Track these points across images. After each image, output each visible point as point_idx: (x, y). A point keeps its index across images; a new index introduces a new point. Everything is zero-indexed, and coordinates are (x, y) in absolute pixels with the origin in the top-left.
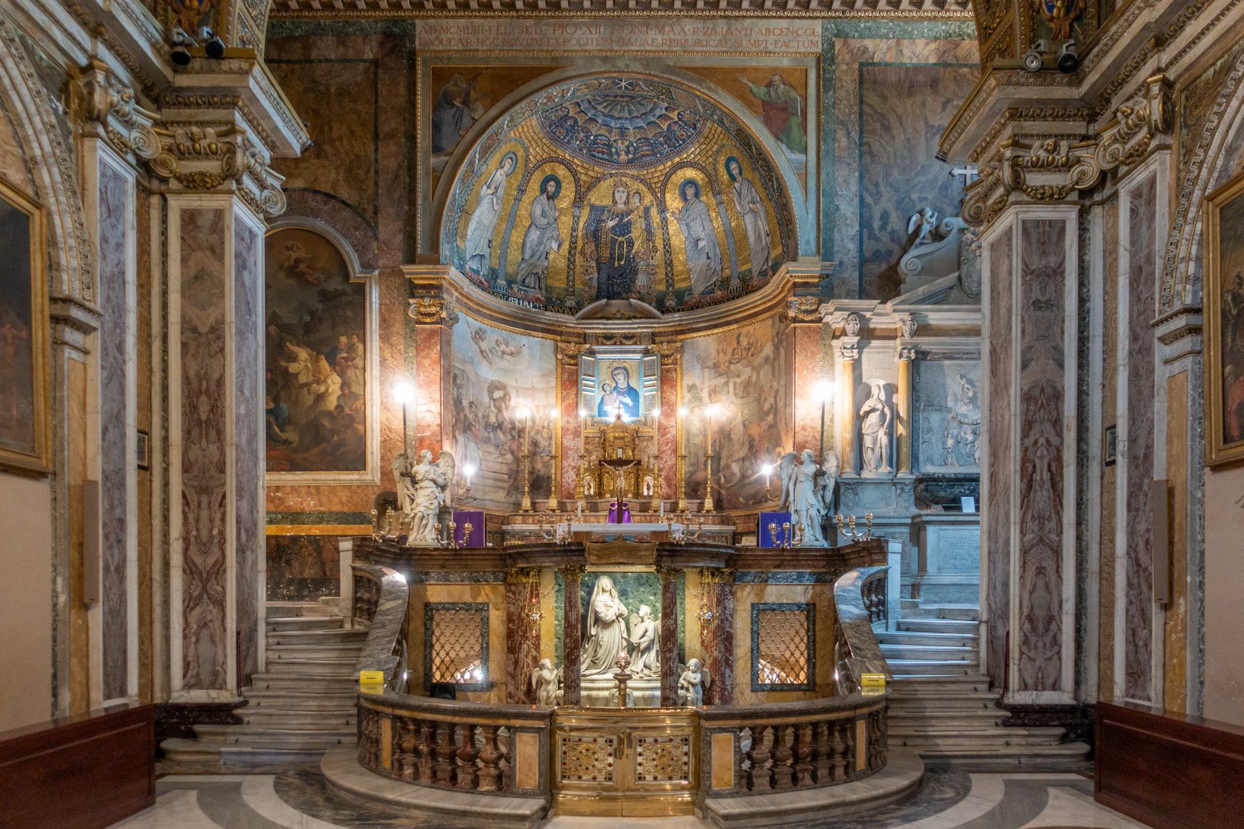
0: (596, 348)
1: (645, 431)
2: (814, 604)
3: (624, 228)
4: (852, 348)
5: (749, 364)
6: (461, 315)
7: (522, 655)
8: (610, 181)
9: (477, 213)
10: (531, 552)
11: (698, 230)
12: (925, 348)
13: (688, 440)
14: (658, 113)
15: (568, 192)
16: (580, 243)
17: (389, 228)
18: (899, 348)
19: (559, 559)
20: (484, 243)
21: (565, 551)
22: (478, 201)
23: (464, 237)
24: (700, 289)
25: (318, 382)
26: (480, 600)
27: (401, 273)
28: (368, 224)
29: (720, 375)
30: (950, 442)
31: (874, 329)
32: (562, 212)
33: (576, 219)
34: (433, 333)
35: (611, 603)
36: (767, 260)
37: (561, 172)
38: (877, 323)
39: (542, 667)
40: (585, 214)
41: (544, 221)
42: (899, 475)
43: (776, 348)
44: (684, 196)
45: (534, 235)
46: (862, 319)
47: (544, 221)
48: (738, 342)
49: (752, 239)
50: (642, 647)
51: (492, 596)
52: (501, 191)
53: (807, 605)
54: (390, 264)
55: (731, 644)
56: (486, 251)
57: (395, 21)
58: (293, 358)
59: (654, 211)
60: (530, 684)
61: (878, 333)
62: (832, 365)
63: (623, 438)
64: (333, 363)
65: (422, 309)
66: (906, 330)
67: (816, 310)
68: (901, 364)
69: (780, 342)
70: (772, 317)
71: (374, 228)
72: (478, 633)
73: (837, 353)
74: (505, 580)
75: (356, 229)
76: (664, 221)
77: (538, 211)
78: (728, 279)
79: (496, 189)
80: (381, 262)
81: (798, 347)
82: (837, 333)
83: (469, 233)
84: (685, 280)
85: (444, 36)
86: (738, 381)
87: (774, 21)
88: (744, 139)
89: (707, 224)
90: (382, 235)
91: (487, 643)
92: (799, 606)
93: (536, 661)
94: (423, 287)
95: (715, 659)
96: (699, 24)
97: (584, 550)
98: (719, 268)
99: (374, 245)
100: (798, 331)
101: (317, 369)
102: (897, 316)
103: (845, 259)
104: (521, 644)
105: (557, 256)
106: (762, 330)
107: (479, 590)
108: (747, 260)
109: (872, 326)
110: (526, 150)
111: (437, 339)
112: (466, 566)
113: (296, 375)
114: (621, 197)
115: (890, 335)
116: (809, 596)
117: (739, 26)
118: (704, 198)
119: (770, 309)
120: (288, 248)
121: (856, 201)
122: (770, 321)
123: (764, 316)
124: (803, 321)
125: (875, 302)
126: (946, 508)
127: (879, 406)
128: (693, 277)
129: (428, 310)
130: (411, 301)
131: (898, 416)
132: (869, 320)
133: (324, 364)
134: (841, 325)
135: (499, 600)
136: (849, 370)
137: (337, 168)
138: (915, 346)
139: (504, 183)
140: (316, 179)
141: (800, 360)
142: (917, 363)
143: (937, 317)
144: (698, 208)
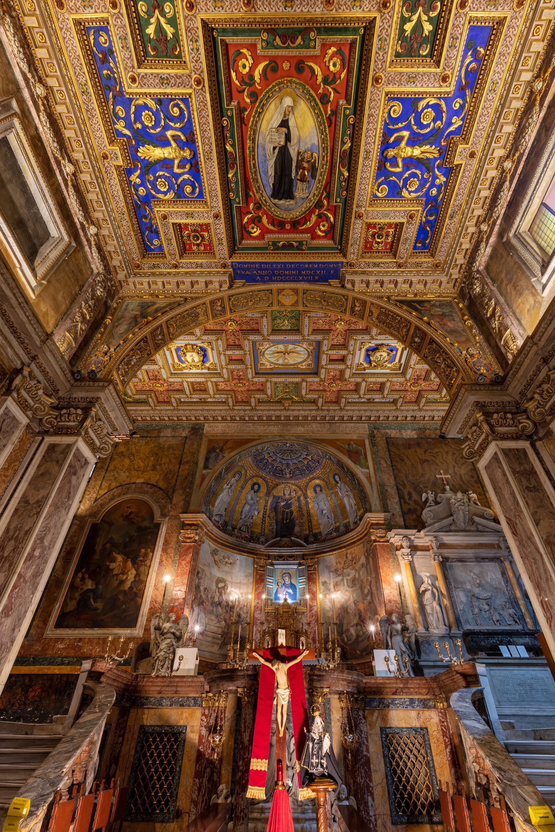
0: (274, 562)
1: (301, 609)
3: (288, 506)
4: (408, 555)
5: (354, 568)
6: (206, 540)
8: (283, 486)
9: (221, 495)
11: (322, 505)
12: (446, 555)
13: (324, 614)
14: (302, 457)
15: (264, 489)
16: (268, 512)
17: (178, 498)
18: (433, 556)
20: (223, 510)
22: (222, 490)
23: (213, 505)
24: (325, 532)
25: (123, 573)
27: (180, 518)
28: (169, 497)
29: (339, 575)
30: (476, 610)
31: (417, 546)
32: (260, 498)
33: (267, 502)
34: (190, 547)
36: (356, 516)
37: (260, 481)
38: (418, 542)
40: (270, 500)
41: (252, 502)
42: (452, 632)
43: (367, 558)
44: (315, 491)
45: (247, 508)
46: (409, 539)
47: (252, 502)
48: (347, 557)
49: (348, 508)
52: (233, 487)
54: (175, 514)
56: (224, 513)
57: (197, 424)
58: (114, 560)
59: (302, 498)
61: (420, 548)
62: (399, 565)
63: (288, 612)
64: (134, 563)
65: (187, 535)
66: (434, 545)
67: (385, 536)
68: (435, 564)
69: (369, 555)
70: (363, 542)
71: (171, 500)
73: (400, 558)
75: (163, 499)
76: (307, 503)
77: (250, 497)
78: (338, 527)
79: (231, 486)
80: (171, 514)
81: (379, 555)
82: (398, 548)
83: (216, 504)
84: (318, 529)
85: (216, 429)
86: (349, 578)
88: (341, 464)
89: (327, 503)
90: (174, 502)
94: (189, 525)
96: (319, 425)
98: (334, 522)
99: (170, 506)
100: (378, 547)
101: (125, 566)
102: (427, 539)
103: (395, 512)
105: (257, 516)
106: (357, 550)
108: (347, 517)
109: (415, 544)
110: (246, 471)
111: (191, 550)
113: (113, 570)
114: (287, 492)
115: (426, 549)
118: (324, 491)
119: (361, 539)
120: (128, 507)
121: (395, 488)
122: (362, 545)
123: (358, 543)
124: (379, 542)
125: (415, 531)
126: (488, 655)
127: (430, 588)
128: (322, 527)
129: (190, 536)
130: (182, 531)
131: (442, 594)
132: (413, 541)
133: (130, 564)
134: (399, 544)
136: (408, 567)
137: (160, 475)
138: (441, 554)
139: (235, 484)
140: (150, 479)
141: (381, 562)
142: (444, 564)
143: (448, 539)
144: (322, 496)
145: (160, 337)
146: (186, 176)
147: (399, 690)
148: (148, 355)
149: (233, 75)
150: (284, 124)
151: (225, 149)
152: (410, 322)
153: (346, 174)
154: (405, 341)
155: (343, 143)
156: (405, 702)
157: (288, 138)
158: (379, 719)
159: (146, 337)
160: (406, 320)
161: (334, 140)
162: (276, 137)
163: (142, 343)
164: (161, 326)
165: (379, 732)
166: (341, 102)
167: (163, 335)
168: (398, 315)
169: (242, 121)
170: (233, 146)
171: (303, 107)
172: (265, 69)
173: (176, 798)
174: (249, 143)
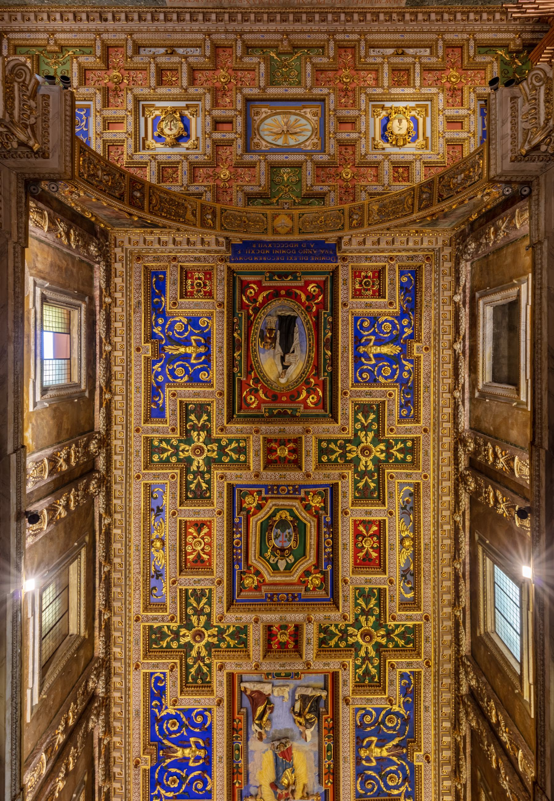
87: (196, 6)
117: (215, 3)
145: (424, 196)
146: (366, 333)
148: (443, 177)
149: (321, 394)
150: (285, 368)
151: (331, 352)
152: (151, 213)
153: (235, 335)
154: (150, 188)
155: (240, 355)
157: (283, 359)
159: (439, 201)
160: (156, 215)
161: (248, 356)
162: (292, 360)
163: (445, 196)
164: (420, 210)
166: (245, 379)
167: (420, 197)
168: (165, 217)
169: (317, 368)
170: (325, 354)
171: (272, 376)
172: (299, 396)
174: (313, 355)
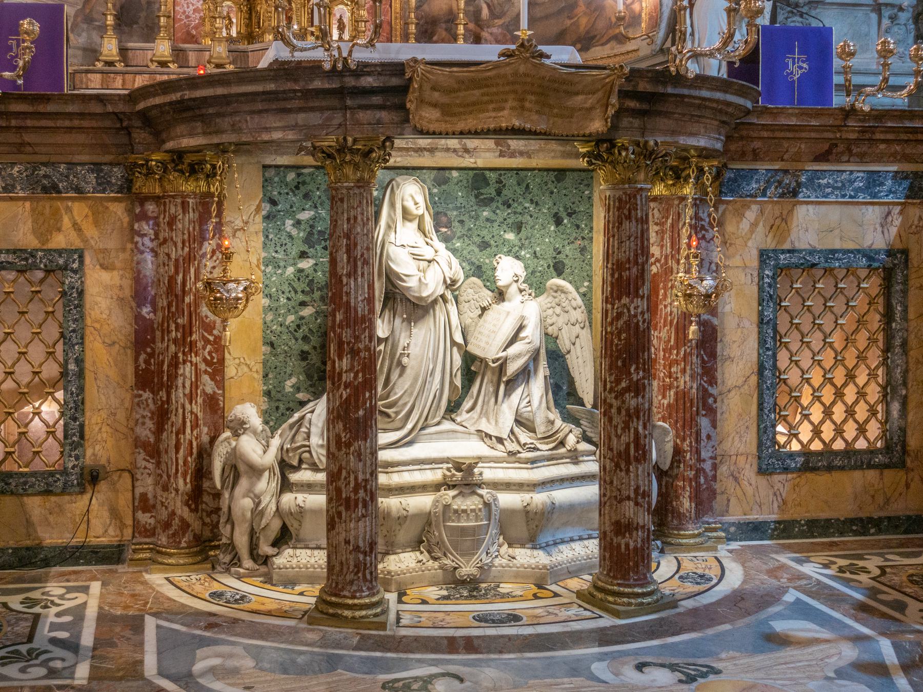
2: (905, 252)
7: (179, 395)
10: (226, 100)
19: (315, 118)
21: (341, 93)
26: (59, 241)
35: (428, 253)
39: (239, 428)
50: (512, 368)
51: (91, 232)
53: (890, 253)
55: (713, 355)
60: (201, 472)
72: (52, 331)
74: (127, 187)
91: (80, 362)
92: (869, 255)
93: (214, 405)
95: (682, 396)
97: (404, 90)
104: (175, 364)
107: (56, 213)
112: (20, 147)
116: (894, 231)
135: (112, 243)
147: (841, 148)
156: (852, 182)
158: (760, 228)
165: (755, 263)
173: (82, 437)
